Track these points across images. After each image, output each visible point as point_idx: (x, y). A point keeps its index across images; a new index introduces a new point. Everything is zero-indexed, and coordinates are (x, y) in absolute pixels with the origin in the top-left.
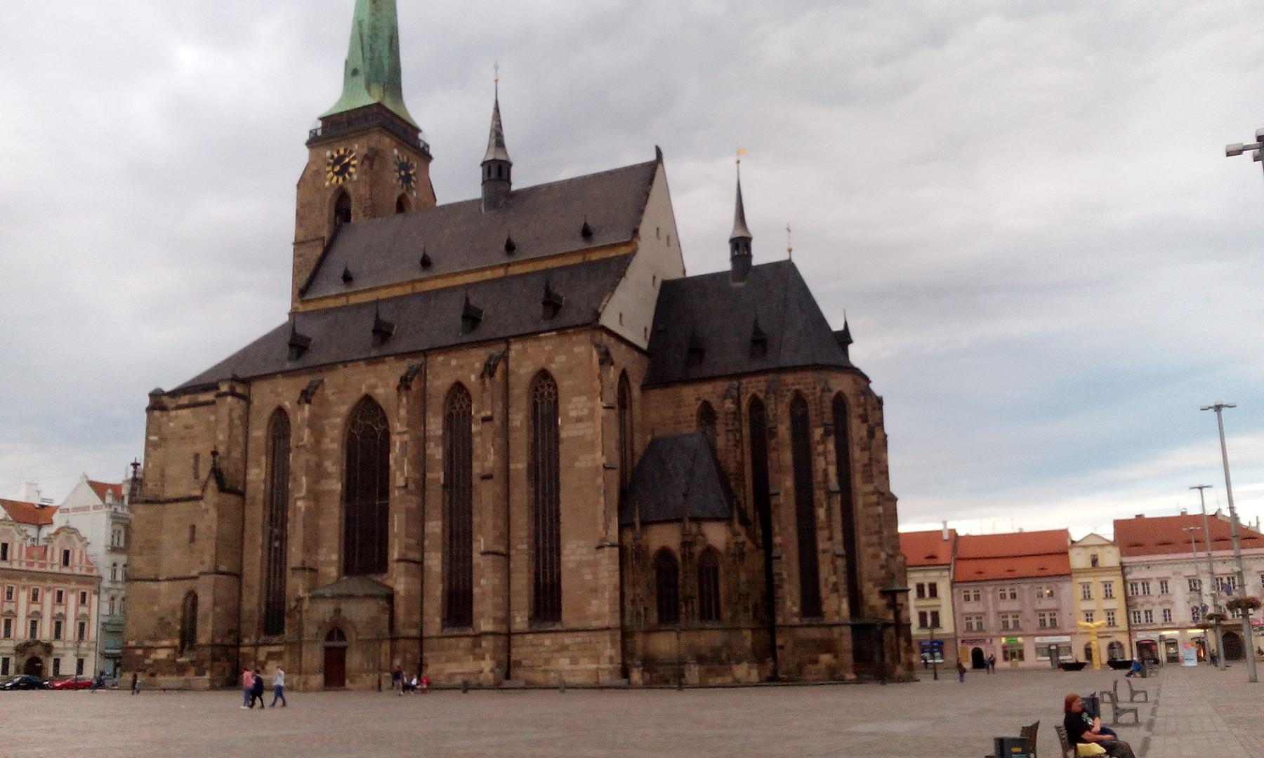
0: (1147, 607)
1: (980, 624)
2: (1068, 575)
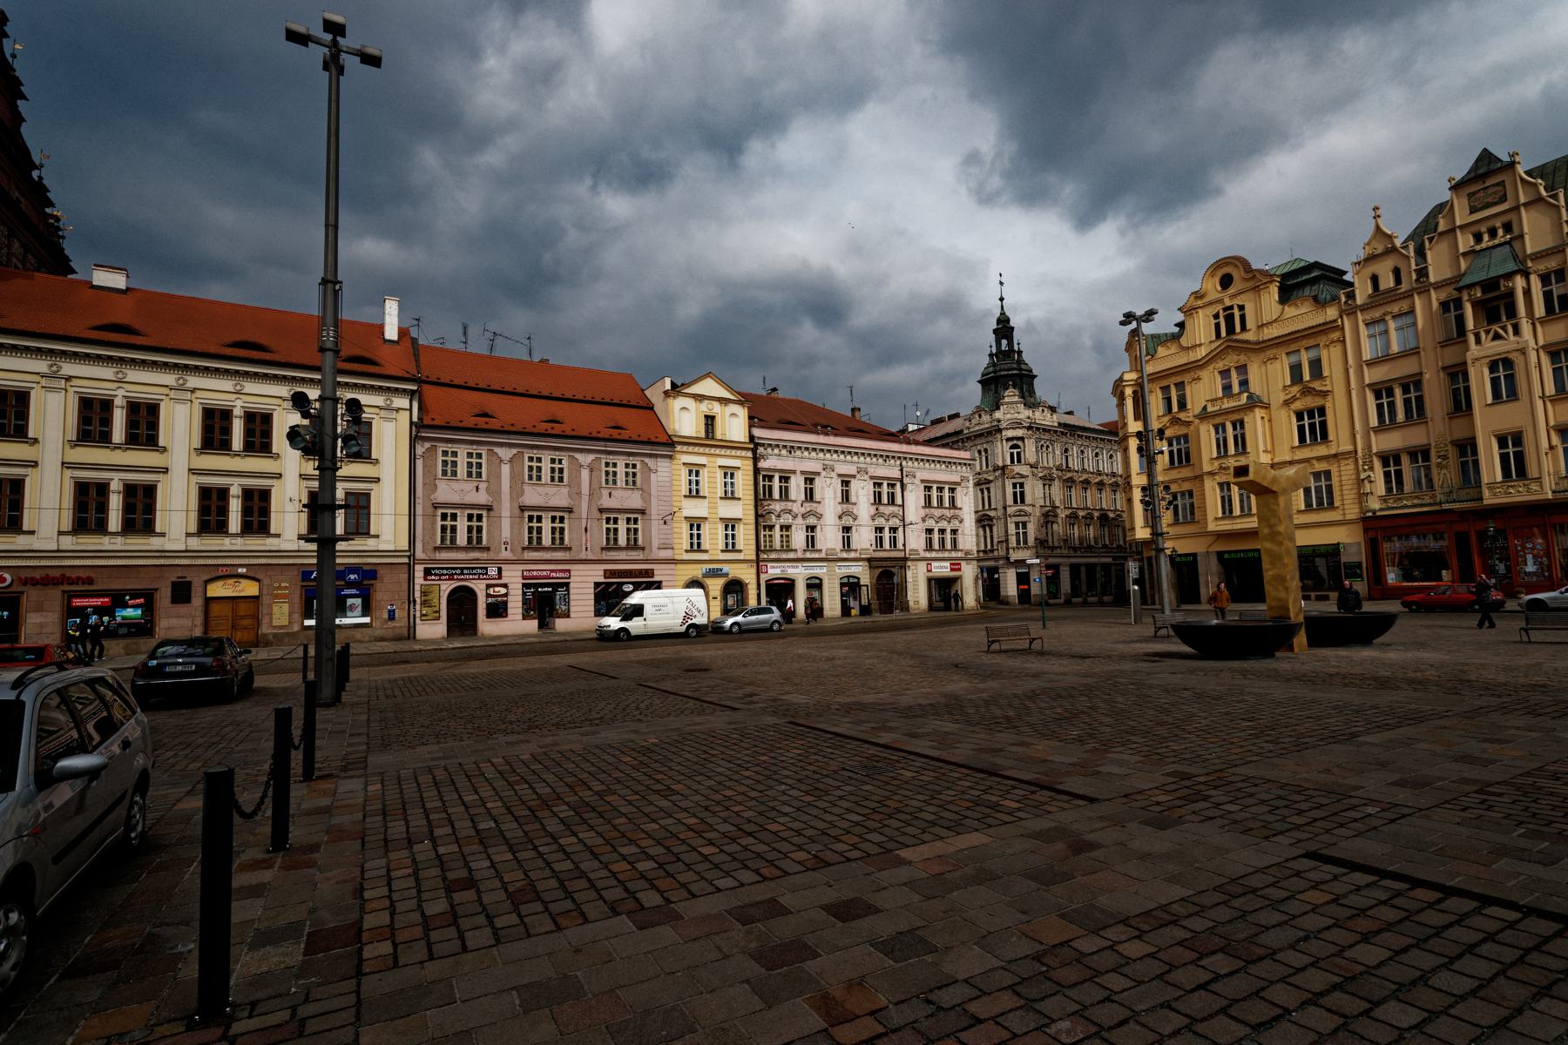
0: (786, 519)
1: (475, 534)
2: (667, 444)
